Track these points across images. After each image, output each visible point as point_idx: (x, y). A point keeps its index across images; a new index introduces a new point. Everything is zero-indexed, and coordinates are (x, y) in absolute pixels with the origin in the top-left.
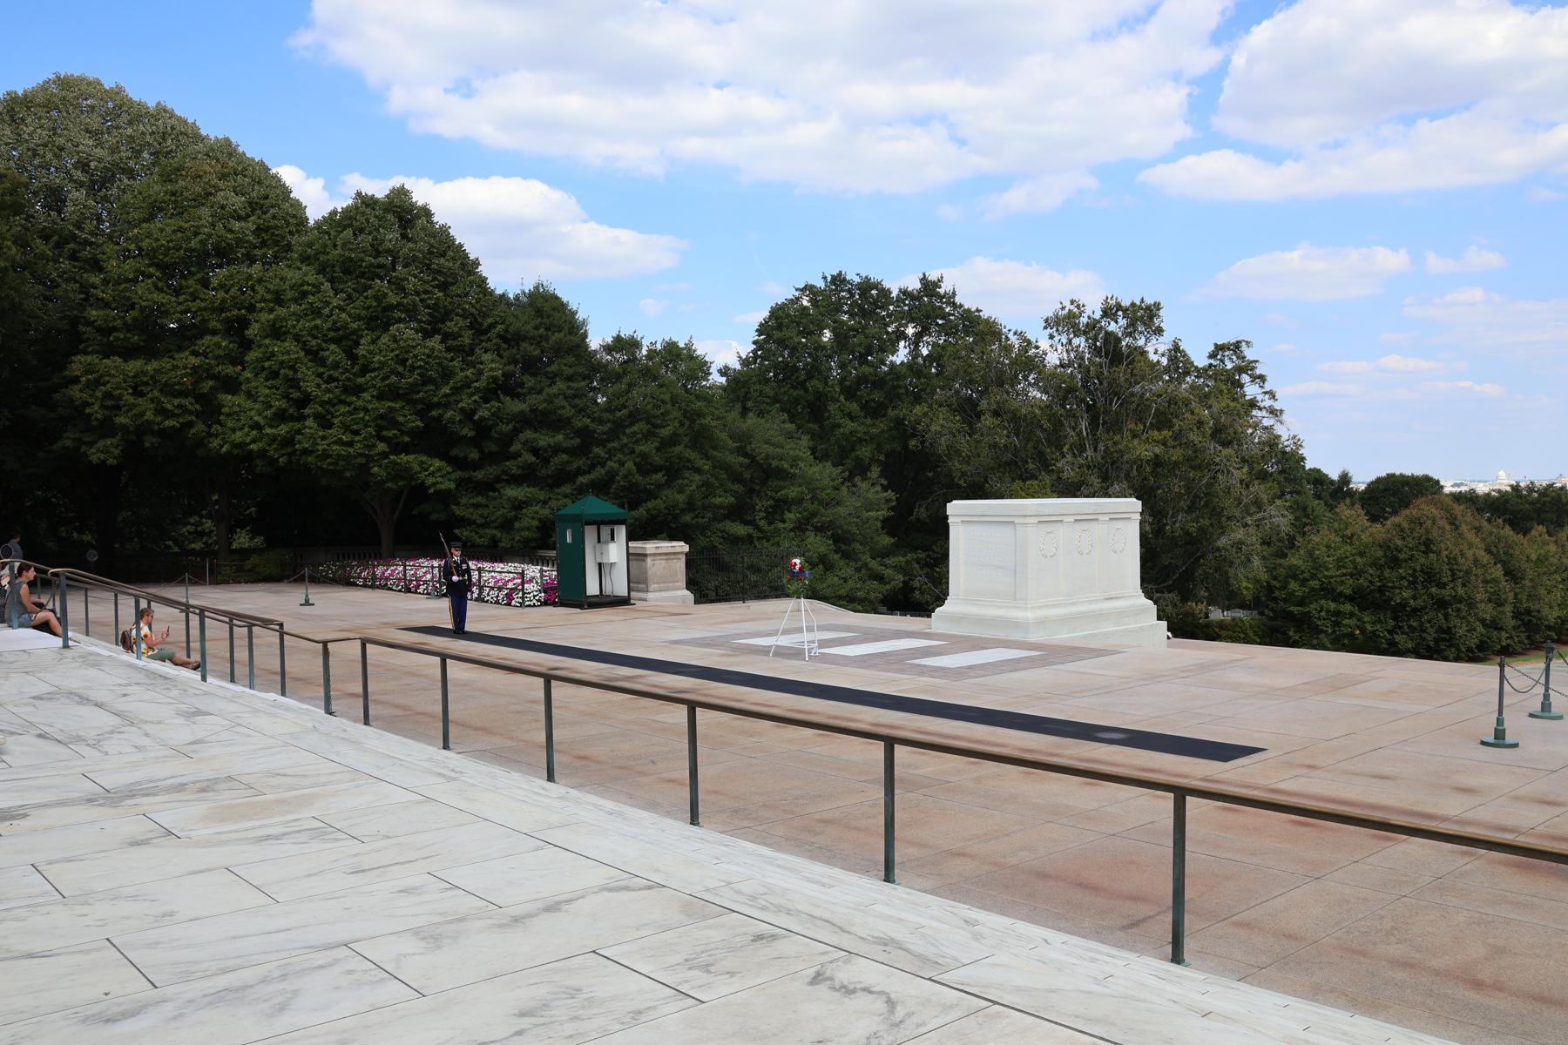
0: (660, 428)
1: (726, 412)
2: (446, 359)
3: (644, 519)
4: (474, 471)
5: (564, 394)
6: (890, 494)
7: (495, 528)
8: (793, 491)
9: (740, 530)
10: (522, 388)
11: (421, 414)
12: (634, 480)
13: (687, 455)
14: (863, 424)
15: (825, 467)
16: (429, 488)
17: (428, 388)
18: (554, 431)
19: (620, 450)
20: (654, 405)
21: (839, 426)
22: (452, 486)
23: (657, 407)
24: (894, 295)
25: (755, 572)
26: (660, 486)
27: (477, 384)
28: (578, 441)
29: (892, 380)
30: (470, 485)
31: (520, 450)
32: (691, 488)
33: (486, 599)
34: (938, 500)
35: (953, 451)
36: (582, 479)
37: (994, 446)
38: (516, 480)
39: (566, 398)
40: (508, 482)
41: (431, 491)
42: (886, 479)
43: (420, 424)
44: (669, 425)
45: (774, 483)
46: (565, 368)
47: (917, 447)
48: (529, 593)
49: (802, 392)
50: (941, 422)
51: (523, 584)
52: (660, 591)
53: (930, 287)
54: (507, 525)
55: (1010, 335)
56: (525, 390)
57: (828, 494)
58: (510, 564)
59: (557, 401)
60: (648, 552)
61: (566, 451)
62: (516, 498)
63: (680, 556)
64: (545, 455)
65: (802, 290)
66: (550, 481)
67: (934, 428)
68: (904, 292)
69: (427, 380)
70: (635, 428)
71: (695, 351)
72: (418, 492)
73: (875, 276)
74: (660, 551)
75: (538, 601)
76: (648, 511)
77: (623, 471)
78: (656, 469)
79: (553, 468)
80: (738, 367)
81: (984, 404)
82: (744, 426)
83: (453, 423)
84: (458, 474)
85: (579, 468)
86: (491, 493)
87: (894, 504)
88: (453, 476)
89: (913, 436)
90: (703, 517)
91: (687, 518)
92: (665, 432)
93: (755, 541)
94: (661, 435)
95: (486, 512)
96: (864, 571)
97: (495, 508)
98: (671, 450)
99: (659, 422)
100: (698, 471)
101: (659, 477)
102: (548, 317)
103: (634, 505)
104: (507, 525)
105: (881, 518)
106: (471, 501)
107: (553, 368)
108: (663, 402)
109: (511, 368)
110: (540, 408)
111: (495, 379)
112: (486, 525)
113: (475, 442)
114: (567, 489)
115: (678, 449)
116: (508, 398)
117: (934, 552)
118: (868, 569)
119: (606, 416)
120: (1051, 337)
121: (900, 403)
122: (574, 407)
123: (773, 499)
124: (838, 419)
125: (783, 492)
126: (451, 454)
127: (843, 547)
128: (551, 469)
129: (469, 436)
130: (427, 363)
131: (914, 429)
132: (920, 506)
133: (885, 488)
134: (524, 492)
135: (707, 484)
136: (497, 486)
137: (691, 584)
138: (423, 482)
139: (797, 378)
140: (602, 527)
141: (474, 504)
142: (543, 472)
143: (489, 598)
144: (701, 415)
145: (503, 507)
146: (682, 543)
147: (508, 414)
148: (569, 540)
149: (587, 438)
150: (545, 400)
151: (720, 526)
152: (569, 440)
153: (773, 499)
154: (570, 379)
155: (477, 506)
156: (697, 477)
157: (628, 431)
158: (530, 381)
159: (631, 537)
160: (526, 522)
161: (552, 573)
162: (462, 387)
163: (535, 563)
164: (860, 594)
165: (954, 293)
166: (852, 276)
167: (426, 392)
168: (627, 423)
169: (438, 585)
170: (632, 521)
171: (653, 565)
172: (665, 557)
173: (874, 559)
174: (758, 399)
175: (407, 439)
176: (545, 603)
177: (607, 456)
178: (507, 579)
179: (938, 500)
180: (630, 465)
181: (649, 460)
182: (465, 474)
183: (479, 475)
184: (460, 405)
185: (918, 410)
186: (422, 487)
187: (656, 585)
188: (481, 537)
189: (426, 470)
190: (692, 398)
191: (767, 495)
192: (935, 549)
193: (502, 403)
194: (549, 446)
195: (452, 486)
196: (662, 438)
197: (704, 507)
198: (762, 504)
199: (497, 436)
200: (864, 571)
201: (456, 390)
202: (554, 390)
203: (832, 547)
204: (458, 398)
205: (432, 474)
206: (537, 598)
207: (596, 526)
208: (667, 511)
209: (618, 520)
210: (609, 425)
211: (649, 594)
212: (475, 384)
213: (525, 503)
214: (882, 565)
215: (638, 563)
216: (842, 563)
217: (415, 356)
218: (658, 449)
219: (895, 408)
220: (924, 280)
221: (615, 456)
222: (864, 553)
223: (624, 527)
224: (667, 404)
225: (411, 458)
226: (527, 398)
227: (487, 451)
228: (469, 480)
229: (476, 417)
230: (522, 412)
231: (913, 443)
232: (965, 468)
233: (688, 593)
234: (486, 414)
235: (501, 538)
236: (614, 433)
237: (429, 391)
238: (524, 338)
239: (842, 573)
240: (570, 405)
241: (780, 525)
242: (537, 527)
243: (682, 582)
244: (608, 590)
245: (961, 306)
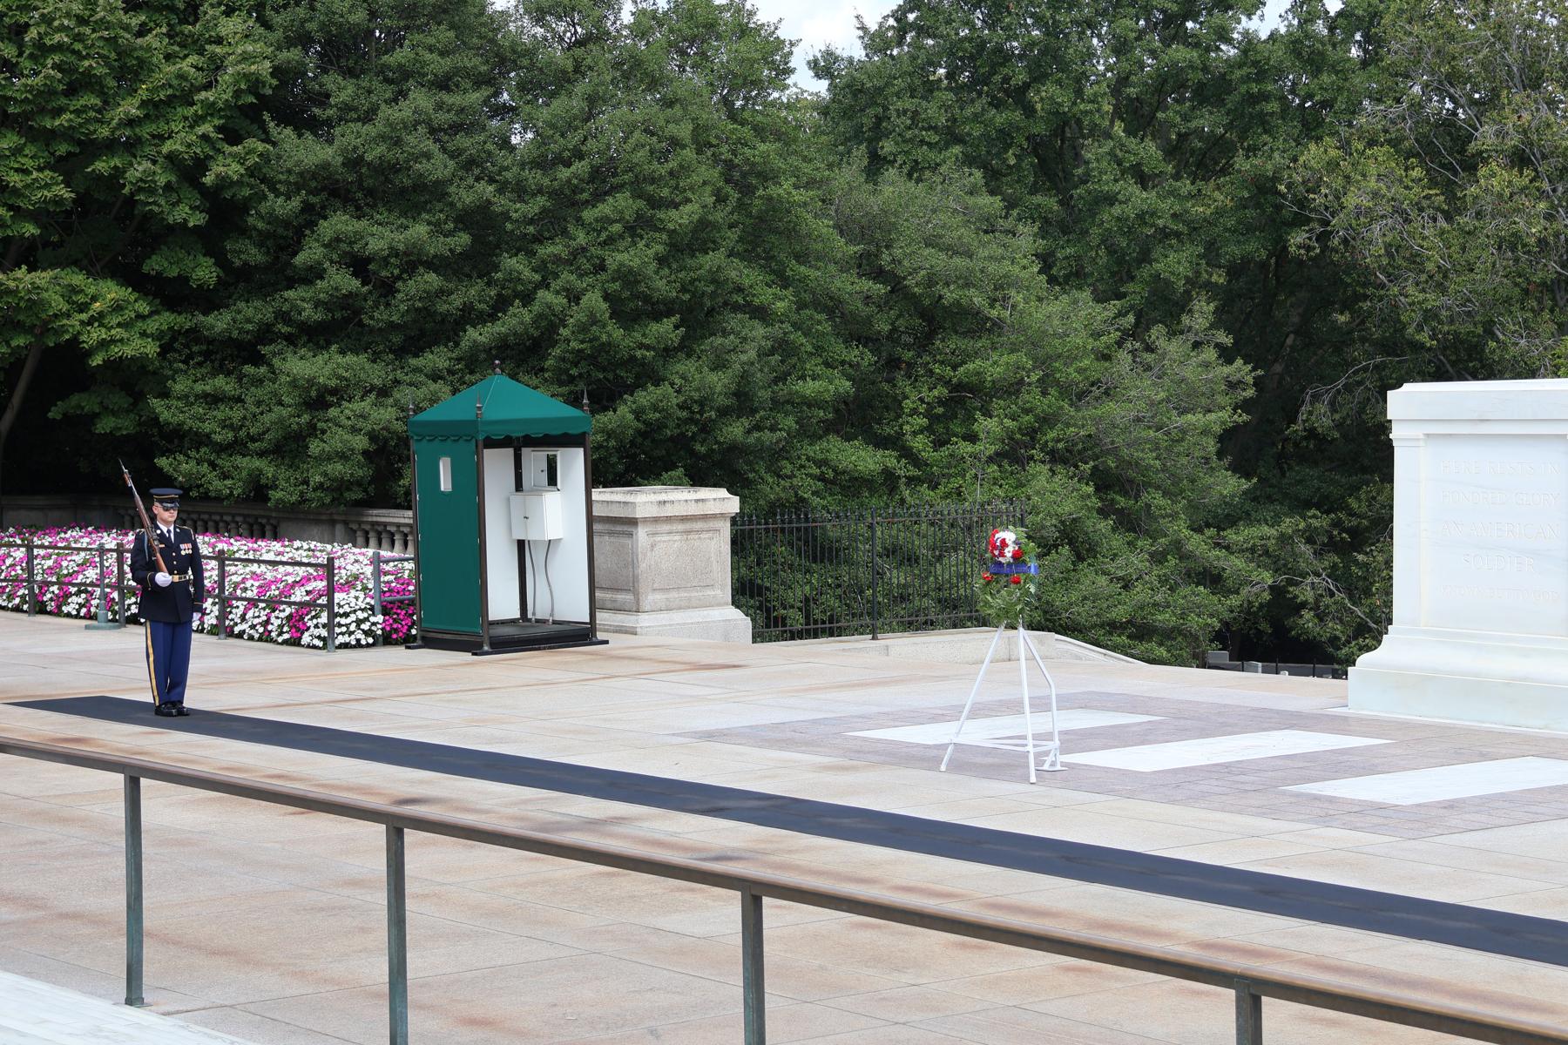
0: (667, 208)
1: (830, 166)
2: (127, 28)
3: (631, 431)
4: (205, 314)
5: (428, 123)
6: (1240, 369)
7: (261, 454)
9: (864, 459)
11: (66, 167)
12: (604, 338)
13: (733, 274)
14: (1173, 193)
15: (1075, 302)
16: (89, 353)
17: (82, 102)
18: (404, 214)
19: (569, 262)
20: (652, 152)
21: (1111, 200)
22: (151, 348)
23: (663, 156)
25: (901, 564)
26: (668, 353)
27: (209, 95)
28: (463, 239)
29: (1247, 79)
30: (196, 349)
31: (320, 263)
32: (744, 358)
33: (237, 630)
34: (1360, 383)
35: (1403, 258)
36: (476, 335)
37: (1512, 243)
38: (315, 336)
39: (433, 131)
40: (291, 340)
41: (97, 360)
42: (1229, 331)
43: (66, 194)
44: (688, 201)
45: (954, 343)
46: (428, 56)
47: (1309, 249)
48: (346, 615)
49: (1017, 116)
50: (1372, 183)
51: (330, 591)
52: (669, 609)
54: (290, 447)
56: (330, 112)
57: (1080, 371)
58: (297, 544)
59: (411, 139)
61: (435, 264)
62: (311, 381)
64: (384, 274)
66: (397, 339)
67: (1351, 201)
69: (78, 84)
70: (605, 209)
71: (751, 14)
74: (669, 511)
75: (367, 633)
76: (638, 413)
77: (577, 315)
78: (659, 310)
79: (403, 307)
80: (858, 53)
81: (1486, 136)
82: (874, 203)
83: (151, 191)
84: (166, 320)
85: (467, 309)
86: (249, 369)
87: (1250, 393)
88: (152, 326)
89: (1299, 221)
90: (773, 429)
91: (735, 430)
92: (682, 217)
93: (903, 487)
94: (671, 226)
95: (236, 414)
96: (1172, 561)
97: (259, 403)
98: (690, 262)
99: (665, 192)
100: (761, 313)
101: (665, 330)
103: (603, 399)
104: (290, 447)
105: (1217, 429)
106: (199, 387)
107: (401, 56)
108: (675, 143)
109: (294, 54)
110: (369, 157)
111: (255, 83)
112: (236, 447)
113: (209, 240)
114: (438, 358)
115: (710, 260)
116: (288, 131)
117: (1352, 514)
118: (1184, 557)
119: (534, 178)
121: (1265, 137)
122: (453, 155)
123: (947, 383)
124: (1108, 181)
125: (971, 366)
126: (146, 269)
127: (1121, 501)
128: (397, 311)
129: (191, 224)
130: (79, 38)
131: (1302, 203)
132: (1316, 398)
133: (1227, 355)
134: (330, 366)
135: (782, 347)
136: (265, 350)
137: (745, 592)
138: (75, 340)
139: (1006, 79)
140: (525, 451)
141: (205, 395)
142: (380, 316)
143: (244, 626)
144: (767, 176)
145: (281, 403)
146: (722, 492)
147: (289, 171)
148: (445, 484)
150: (383, 137)
151: (815, 450)
152: (442, 239)
153: (947, 383)
154: (443, 84)
155: (214, 400)
156: (759, 331)
157: (588, 215)
158: (342, 90)
160: (337, 439)
161: (401, 564)
162: (170, 102)
163: (360, 540)
164: (1164, 618)
167: (77, 112)
168: (585, 196)
169: (115, 595)
170: (599, 438)
171: (653, 546)
172: (681, 527)
173: (1199, 530)
174: (909, 134)
175: (30, 230)
176: (386, 640)
177: (537, 277)
178: (290, 580)
179: (1360, 383)
180: (594, 300)
181: (642, 288)
182: (182, 321)
183: (218, 323)
184: (167, 147)
185: (1313, 154)
186: (73, 351)
187: (658, 596)
188: (225, 476)
189: (83, 308)
190: (746, 132)
191: (931, 372)
192: (1354, 504)
193: (274, 144)
194: (394, 252)
195: (151, 348)
196: (672, 233)
197: (777, 404)
198: (917, 396)
199: (260, 225)
200: (1172, 561)
201: (155, 109)
202: (403, 112)
203: (1095, 502)
204: (162, 128)
205: (99, 318)
206: (365, 626)
207: (511, 451)
208: (685, 414)
209: (565, 435)
210: (541, 201)
211: (642, 616)
212: (203, 95)
213: (334, 391)
214: (1217, 545)
215: (612, 539)
216: (1118, 541)
217: (47, 20)
218: (662, 261)
219: (1252, 150)
221: (556, 276)
222: (1174, 516)
223: (581, 451)
224: (684, 147)
225: (42, 277)
226: (337, 131)
227: (237, 263)
228: (194, 334)
229: (209, 179)
230: (325, 166)
231: (1299, 240)
232: (1432, 299)
233: (737, 614)
234: (234, 170)
235: (275, 478)
236: (553, 222)
237: (84, 109)
239: (1118, 568)
240: (444, 150)
241: (965, 448)
242: (365, 453)
243: (723, 588)
244: (540, 608)
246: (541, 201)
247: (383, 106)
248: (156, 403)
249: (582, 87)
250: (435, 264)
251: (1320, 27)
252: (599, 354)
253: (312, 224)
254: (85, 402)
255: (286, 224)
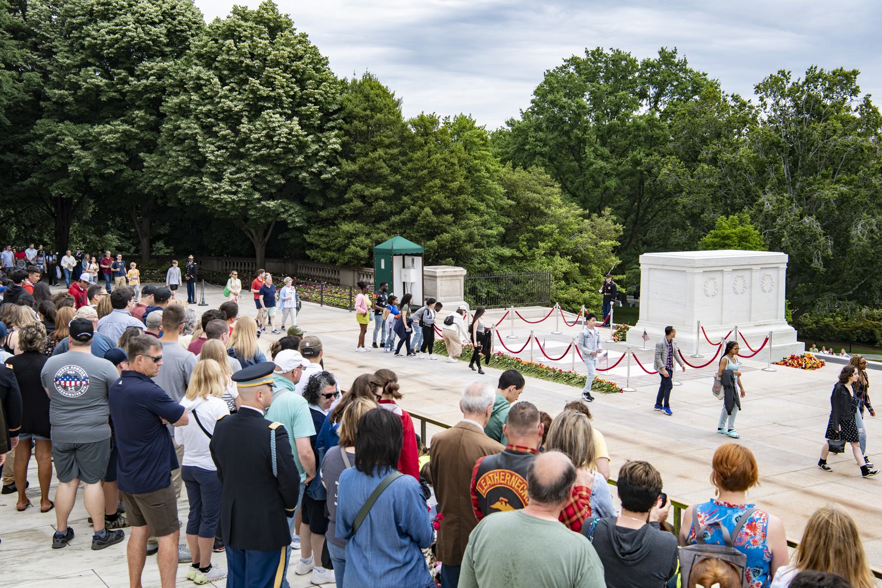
6: (619, 227)
8: (546, 227)
10: (354, 154)
24: (639, 63)
28: (393, 191)
36: (393, 219)
39: (384, 161)
40: (344, 219)
45: (535, 219)
46: (384, 139)
53: (667, 57)
55: (729, 99)
60: (437, 275)
61: (384, 199)
62: (348, 232)
63: (460, 278)
65: (569, 61)
68: (647, 64)
70: (431, 183)
72: (282, 226)
73: (625, 50)
74: (446, 274)
78: (447, 212)
86: (331, 227)
87: (622, 233)
92: (455, 185)
95: (326, 240)
99: (450, 178)
101: (449, 218)
102: (373, 101)
103: (431, 236)
104: (341, 249)
114: (383, 226)
115: (462, 197)
120: (761, 99)
122: (389, 167)
128: (373, 211)
136: (336, 222)
140: (406, 257)
146: (462, 269)
148: (383, 267)
149: (400, 190)
150: (369, 162)
153: (532, 231)
155: (321, 235)
159: (426, 263)
165: (685, 61)
166: (606, 51)
183: (323, 214)
194: (372, 195)
196: (451, 190)
202: (376, 154)
210: (414, 181)
213: (354, 234)
220: (662, 52)
236: (418, 187)
238: (355, 118)
239: (580, 286)
240: (387, 165)
245: (691, 71)
246: (414, 181)
247: (370, 153)
248: (306, 236)
249: (426, 148)
250: (384, 199)
251: (658, 115)
252: (429, 225)
253: (349, 186)
254: (287, 235)
255: (343, 186)
